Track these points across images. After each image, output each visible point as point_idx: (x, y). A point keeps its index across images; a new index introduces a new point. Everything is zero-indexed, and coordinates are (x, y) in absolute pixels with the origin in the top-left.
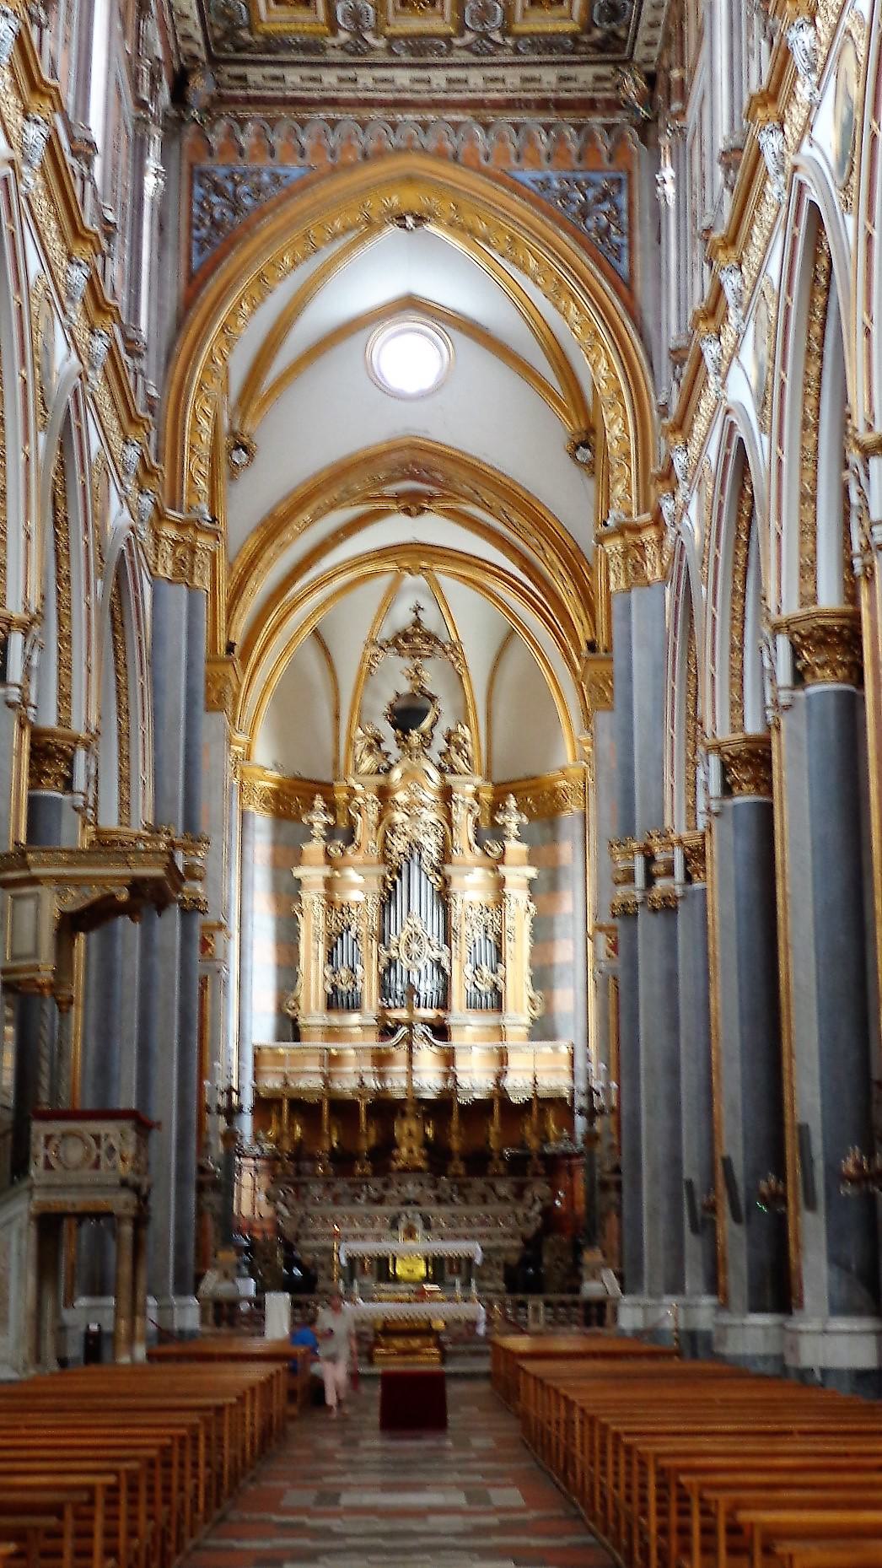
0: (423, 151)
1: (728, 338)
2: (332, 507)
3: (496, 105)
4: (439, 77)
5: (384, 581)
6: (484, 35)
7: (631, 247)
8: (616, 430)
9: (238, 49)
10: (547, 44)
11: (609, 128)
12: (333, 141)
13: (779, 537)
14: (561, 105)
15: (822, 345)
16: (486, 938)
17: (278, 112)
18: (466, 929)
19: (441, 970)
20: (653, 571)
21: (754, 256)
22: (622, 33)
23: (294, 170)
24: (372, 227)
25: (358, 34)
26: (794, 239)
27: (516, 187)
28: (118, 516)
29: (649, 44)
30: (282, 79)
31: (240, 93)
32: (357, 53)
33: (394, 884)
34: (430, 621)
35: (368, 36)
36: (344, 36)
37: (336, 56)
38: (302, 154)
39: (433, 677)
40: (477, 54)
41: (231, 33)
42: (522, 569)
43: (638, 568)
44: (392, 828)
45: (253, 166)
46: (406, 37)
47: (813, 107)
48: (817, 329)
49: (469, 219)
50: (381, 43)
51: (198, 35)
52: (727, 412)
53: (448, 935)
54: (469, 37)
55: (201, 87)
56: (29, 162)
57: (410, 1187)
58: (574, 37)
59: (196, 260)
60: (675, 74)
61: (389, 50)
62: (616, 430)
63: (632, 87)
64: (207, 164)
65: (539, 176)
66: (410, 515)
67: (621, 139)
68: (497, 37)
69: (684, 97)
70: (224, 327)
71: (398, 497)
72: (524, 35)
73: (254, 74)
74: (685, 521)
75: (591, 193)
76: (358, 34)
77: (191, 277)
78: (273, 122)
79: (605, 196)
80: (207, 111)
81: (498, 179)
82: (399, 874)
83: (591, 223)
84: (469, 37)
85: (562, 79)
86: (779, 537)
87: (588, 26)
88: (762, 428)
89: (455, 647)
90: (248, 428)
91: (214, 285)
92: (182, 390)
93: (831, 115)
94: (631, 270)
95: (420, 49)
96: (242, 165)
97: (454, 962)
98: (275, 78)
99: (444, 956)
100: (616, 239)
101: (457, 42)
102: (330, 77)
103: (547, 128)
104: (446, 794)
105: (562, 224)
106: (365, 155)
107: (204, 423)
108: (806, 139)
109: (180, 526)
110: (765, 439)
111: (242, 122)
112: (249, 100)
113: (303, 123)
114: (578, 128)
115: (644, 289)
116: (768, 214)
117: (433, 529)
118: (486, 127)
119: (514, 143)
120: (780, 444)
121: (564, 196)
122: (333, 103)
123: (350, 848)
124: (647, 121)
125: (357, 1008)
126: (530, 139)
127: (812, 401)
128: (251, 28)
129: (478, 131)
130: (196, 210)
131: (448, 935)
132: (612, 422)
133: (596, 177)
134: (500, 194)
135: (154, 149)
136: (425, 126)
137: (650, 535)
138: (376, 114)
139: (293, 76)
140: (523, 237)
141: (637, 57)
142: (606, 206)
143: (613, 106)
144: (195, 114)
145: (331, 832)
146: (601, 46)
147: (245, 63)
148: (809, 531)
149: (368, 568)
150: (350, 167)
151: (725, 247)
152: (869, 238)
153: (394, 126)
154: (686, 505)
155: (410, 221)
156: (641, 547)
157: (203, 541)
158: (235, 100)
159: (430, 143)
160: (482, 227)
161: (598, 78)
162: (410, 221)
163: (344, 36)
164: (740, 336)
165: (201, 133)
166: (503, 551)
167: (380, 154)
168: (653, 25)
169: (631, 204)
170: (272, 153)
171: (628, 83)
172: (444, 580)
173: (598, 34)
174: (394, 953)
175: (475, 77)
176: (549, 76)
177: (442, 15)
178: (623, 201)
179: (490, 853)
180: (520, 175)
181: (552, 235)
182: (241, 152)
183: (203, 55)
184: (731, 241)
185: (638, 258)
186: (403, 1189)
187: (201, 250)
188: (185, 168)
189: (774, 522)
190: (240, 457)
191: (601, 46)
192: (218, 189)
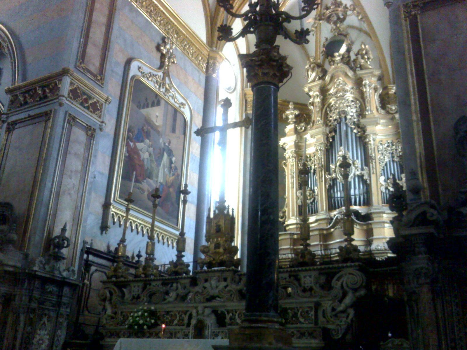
16: (393, 161)
18: (379, 156)
19: (365, 182)
33: (333, 138)
44: (329, 106)
53: (367, 160)
57: (213, 282)
82: (335, 131)
97: (373, 177)
99: (365, 173)
104: (359, 83)
123: (309, 126)
125: (315, 213)
131: (367, 160)
145: (298, 119)
174: (334, 175)
179: (391, 112)
186: (207, 285)
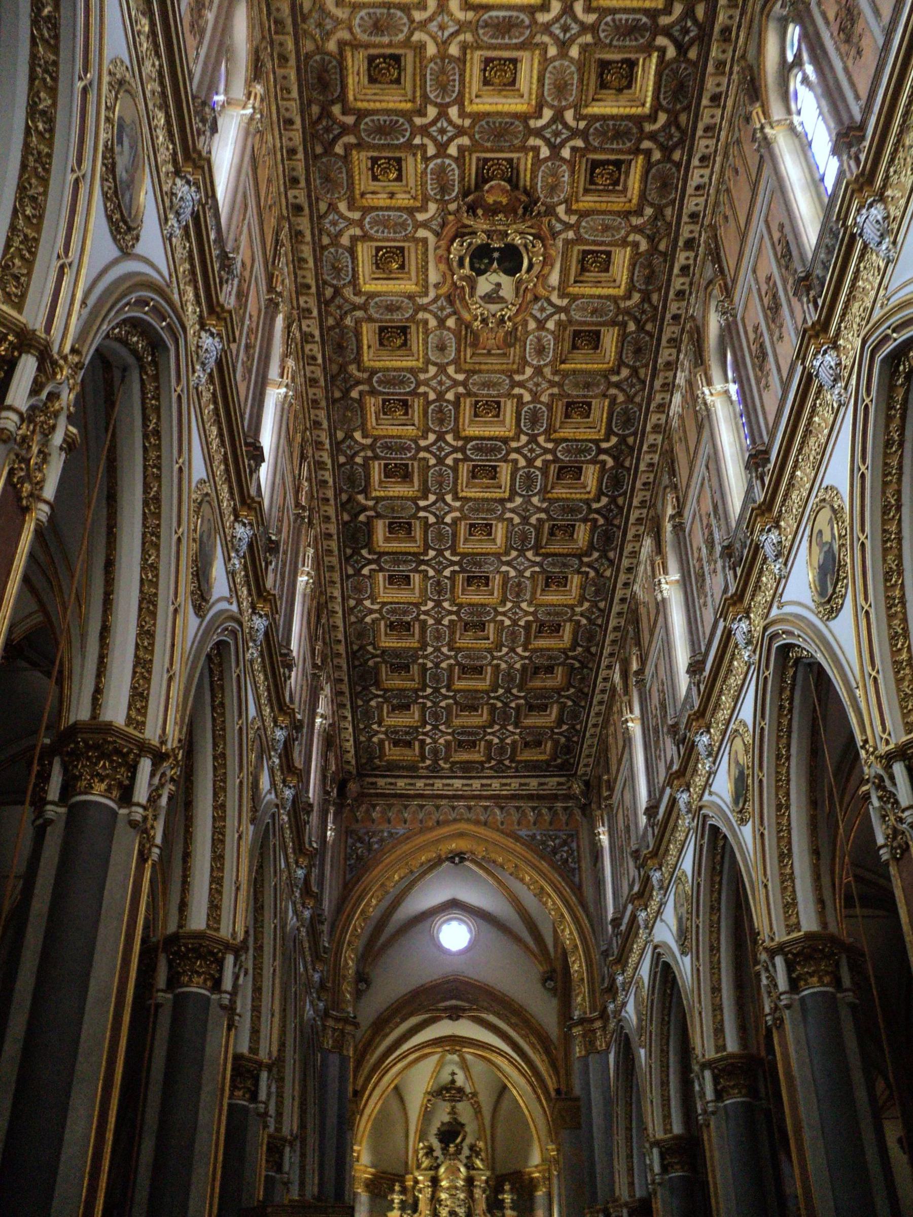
0: (468, 820)
1: (654, 905)
2: (412, 1014)
3: (506, 797)
4: (476, 784)
5: (436, 1058)
6: (500, 762)
7: (580, 867)
8: (576, 967)
9: (374, 769)
10: (534, 768)
11: (565, 809)
12: (421, 816)
13: (700, 1013)
14: (540, 797)
15: (719, 903)
17: (393, 801)
20: (600, 1044)
21: (671, 860)
22: (572, 761)
23: (401, 830)
24: (439, 861)
25: (435, 761)
26: (701, 846)
27: (517, 839)
28: (309, 1012)
29: (586, 765)
30: (395, 784)
31: (372, 791)
32: (435, 772)
34: (460, 1080)
35: (441, 762)
36: (428, 762)
37: (424, 772)
38: (405, 822)
39: (465, 1111)
40: (496, 771)
41: (371, 759)
42: (514, 1050)
43: (592, 1043)
45: (381, 827)
46: (461, 762)
47: (711, 774)
48: (716, 895)
49: (493, 856)
50: (447, 766)
51: (353, 762)
52: (656, 947)
54: (493, 763)
55: (353, 787)
56: (284, 808)
58: (547, 763)
59: (348, 877)
60: (605, 777)
61: (451, 769)
62: (576, 967)
63: (577, 788)
64: (355, 827)
65: (530, 833)
66: (544, 981)
67: (571, 815)
68: (507, 762)
69: (611, 789)
70: (363, 912)
71: (445, 1009)
72: (521, 761)
73: (381, 782)
74: (623, 1014)
75: (557, 841)
76: (435, 761)
77: (345, 885)
78: (390, 806)
79: (565, 843)
80: (355, 800)
81: (508, 835)
83: (558, 857)
84: (493, 763)
85: (541, 784)
86: (700, 1013)
87: (554, 757)
88: (683, 953)
89: (474, 1094)
90: (367, 970)
91: (359, 888)
92: (340, 944)
93: (726, 776)
94: (580, 880)
95: (468, 769)
96: (374, 827)
98: (391, 784)
100: (572, 865)
101: (487, 765)
102: (420, 784)
103: (534, 809)
105: (542, 858)
106: (438, 822)
107: (351, 963)
108: (707, 792)
109: (337, 1020)
110: (687, 960)
111: (374, 806)
112: (377, 795)
113: (406, 807)
114: (550, 809)
115: (589, 891)
116: (680, 836)
117: (465, 1028)
118: (502, 808)
119: (515, 817)
120: (698, 959)
121: (543, 843)
122: (422, 796)
124: (585, 805)
126: (524, 814)
127: (715, 935)
128: (380, 758)
129: (497, 811)
130: (349, 851)
132: (574, 962)
133: (561, 834)
134: (510, 843)
135: (330, 818)
136: (469, 808)
137: (598, 1024)
138: (444, 802)
139: (401, 783)
140: (522, 865)
141: (579, 773)
142: (566, 848)
143: (568, 797)
144: (349, 801)
146: (561, 767)
147: (376, 776)
148: (717, 1008)
149: (427, 1051)
150: (431, 829)
151: (651, 858)
152: (762, 835)
153: (453, 808)
154: (624, 1004)
155: (457, 860)
156: (594, 1031)
157: (349, 1028)
158: (370, 795)
159: (472, 816)
160: (500, 860)
161: (559, 784)
162: (457, 860)
163: (428, 762)
164: (662, 904)
165: (352, 810)
166: (504, 1040)
167: (447, 822)
168: (589, 756)
169: (578, 846)
170: (389, 822)
171: (575, 786)
172: (468, 1057)
173: (559, 761)
175: (496, 784)
176: (534, 783)
177: (479, 752)
178: (574, 845)
180: (520, 833)
181: (538, 864)
182: (373, 821)
183: (354, 772)
184: (655, 854)
185: (584, 876)
187: (351, 871)
188: (343, 829)
189: (697, 1005)
190: (362, 986)
191: (561, 767)
192: (360, 840)
